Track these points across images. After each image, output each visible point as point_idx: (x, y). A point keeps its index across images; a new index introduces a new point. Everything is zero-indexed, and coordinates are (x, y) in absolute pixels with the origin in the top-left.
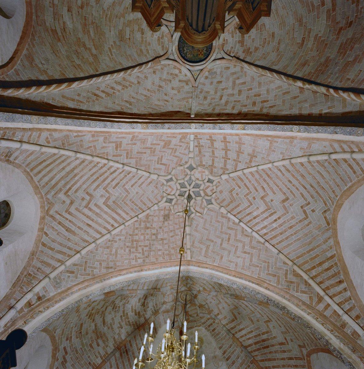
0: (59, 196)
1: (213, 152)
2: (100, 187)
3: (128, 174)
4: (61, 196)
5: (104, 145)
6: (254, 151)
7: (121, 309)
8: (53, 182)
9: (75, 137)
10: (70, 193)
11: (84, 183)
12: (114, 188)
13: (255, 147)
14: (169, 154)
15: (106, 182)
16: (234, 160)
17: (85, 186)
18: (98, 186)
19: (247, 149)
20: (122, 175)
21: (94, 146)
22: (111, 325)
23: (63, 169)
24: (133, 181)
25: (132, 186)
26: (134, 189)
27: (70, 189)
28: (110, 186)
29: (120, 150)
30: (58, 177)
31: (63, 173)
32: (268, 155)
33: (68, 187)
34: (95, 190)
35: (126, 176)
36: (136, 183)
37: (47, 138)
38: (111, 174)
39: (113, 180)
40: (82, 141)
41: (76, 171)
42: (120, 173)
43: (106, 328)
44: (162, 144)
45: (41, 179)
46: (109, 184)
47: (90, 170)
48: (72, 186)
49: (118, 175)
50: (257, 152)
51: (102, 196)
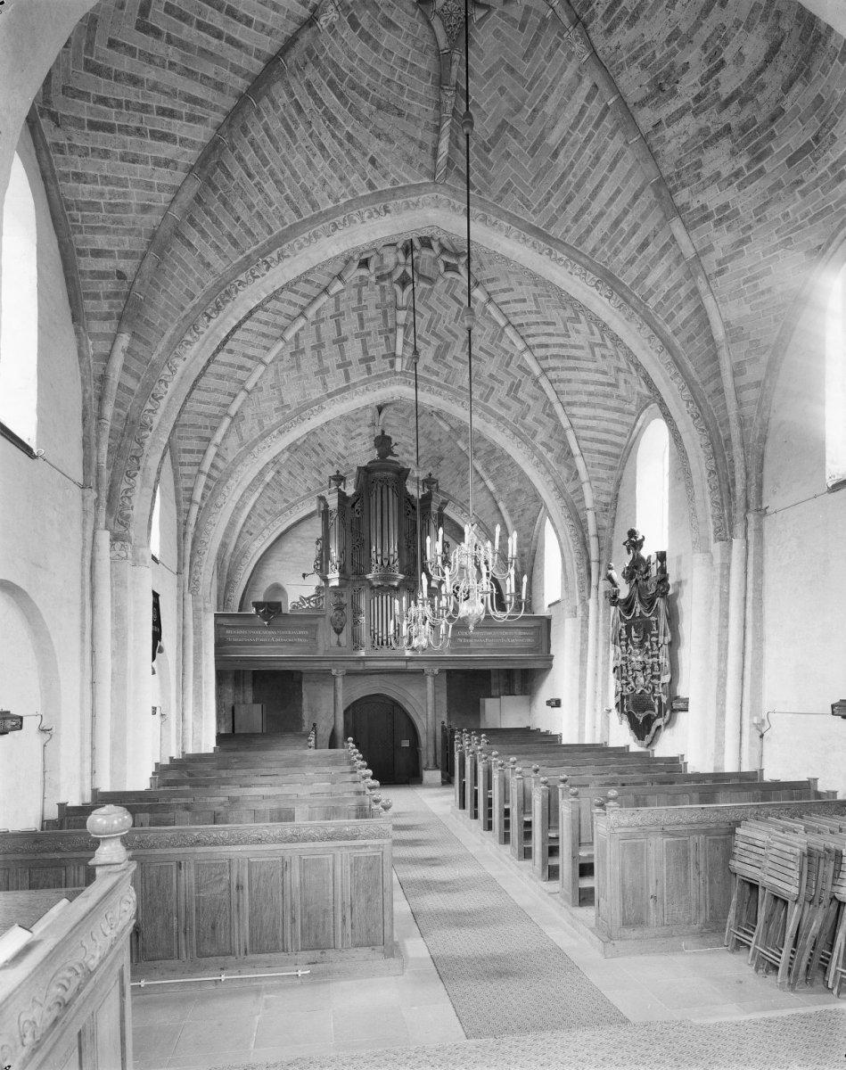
0: (625, 394)
1: (362, 326)
2: (573, 343)
3: (522, 325)
4: (622, 391)
5: (531, 402)
6: (299, 366)
7: (705, 32)
8: (616, 416)
9: (550, 450)
10: (613, 381)
11: (590, 370)
12: (554, 324)
13: (300, 378)
14: (441, 322)
15: (561, 340)
16: (323, 320)
17: (592, 365)
18: (574, 347)
19: (308, 362)
20: (532, 330)
21: (543, 412)
22: (765, 17)
23: (594, 418)
24: (519, 307)
25: (524, 301)
26: (522, 293)
27: (609, 385)
28: (558, 332)
29: (516, 378)
30: (607, 414)
31: (599, 412)
32: (277, 371)
33: (608, 389)
34: (582, 348)
35: (527, 324)
36: (515, 301)
37: (574, 479)
38: (547, 346)
39: (550, 335)
40: (551, 437)
41: (585, 398)
42: (533, 336)
43: (786, 25)
44: (449, 358)
45: (621, 435)
46: (558, 335)
47: (569, 381)
48: (602, 384)
49: (538, 335)
50: (293, 367)
51: (578, 332)
